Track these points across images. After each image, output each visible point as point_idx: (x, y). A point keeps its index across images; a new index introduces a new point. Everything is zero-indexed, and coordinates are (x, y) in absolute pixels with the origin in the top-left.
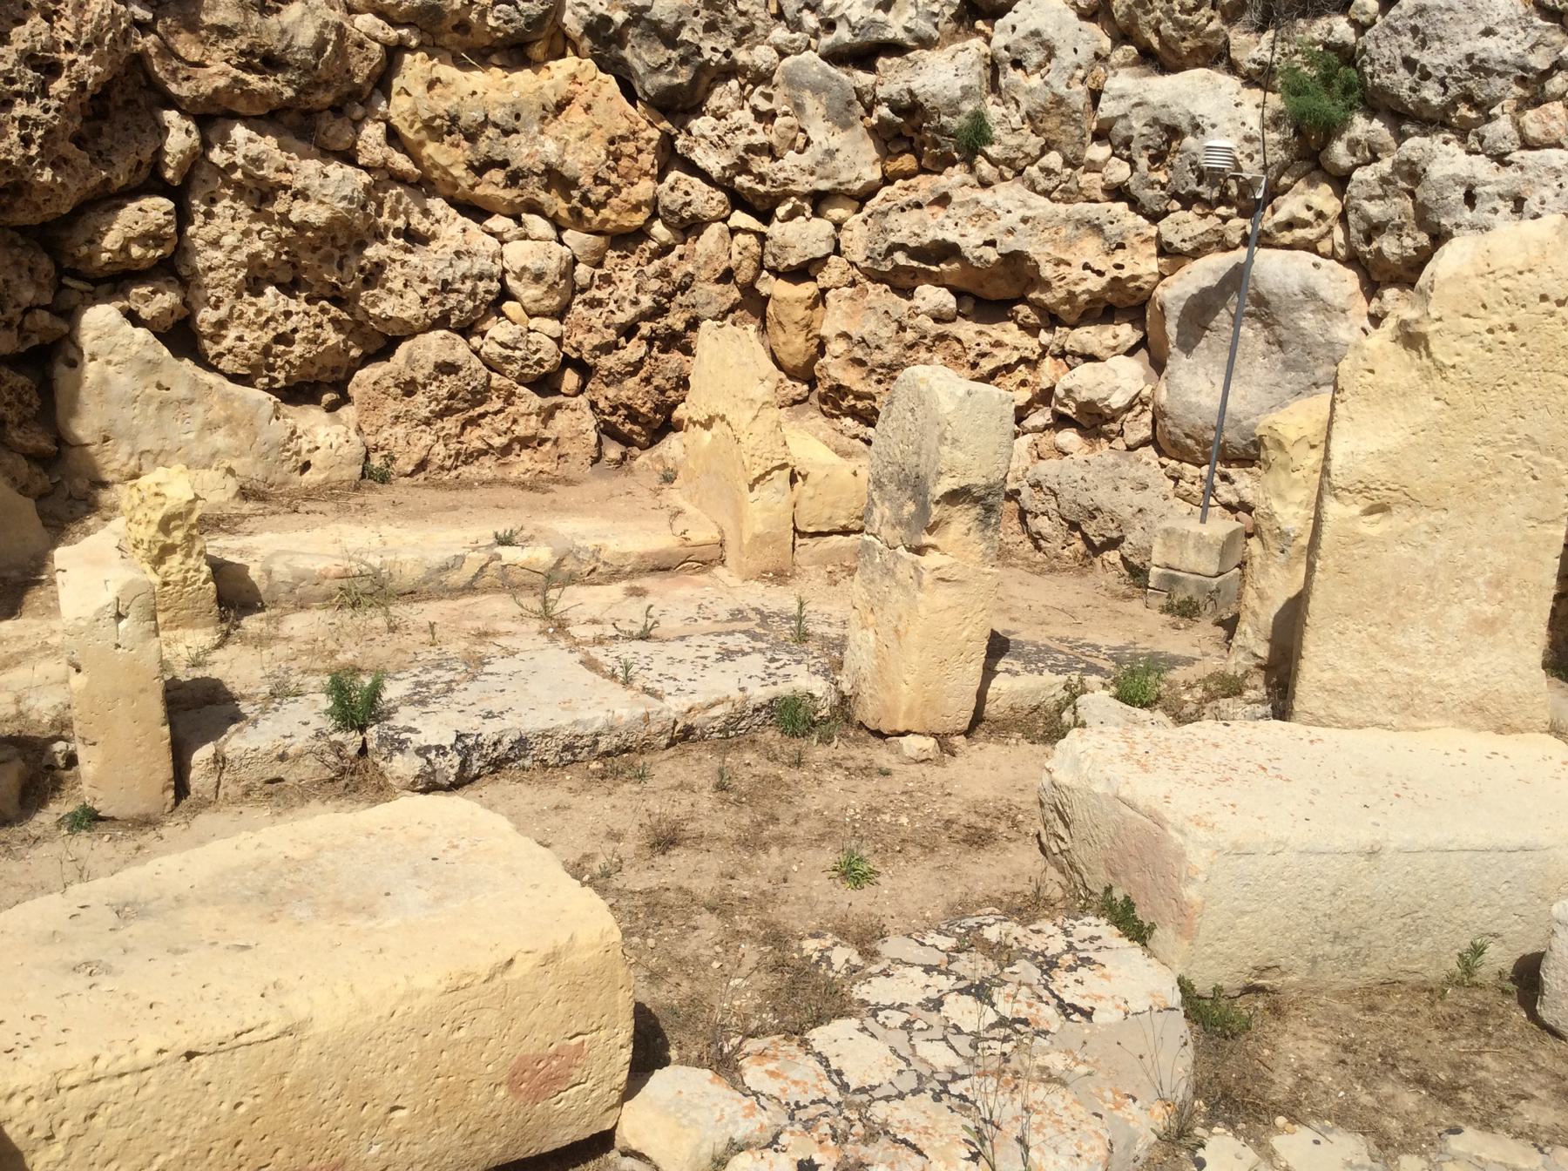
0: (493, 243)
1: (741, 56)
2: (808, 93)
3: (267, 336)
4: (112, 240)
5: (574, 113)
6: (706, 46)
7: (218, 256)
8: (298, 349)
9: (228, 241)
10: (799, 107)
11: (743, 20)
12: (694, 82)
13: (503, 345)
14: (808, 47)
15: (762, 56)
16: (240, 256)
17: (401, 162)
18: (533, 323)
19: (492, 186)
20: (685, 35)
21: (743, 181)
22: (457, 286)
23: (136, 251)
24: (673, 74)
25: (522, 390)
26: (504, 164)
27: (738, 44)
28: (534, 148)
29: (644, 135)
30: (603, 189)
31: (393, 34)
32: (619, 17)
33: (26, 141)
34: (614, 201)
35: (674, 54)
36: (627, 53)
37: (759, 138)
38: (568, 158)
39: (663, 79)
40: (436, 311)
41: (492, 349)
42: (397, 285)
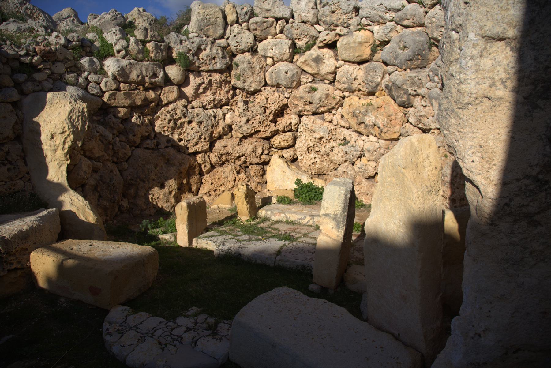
0: (361, 142)
1: (419, 91)
2: (434, 100)
3: (310, 163)
4: (278, 141)
5: (382, 110)
6: (410, 89)
7: (301, 144)
8: (317, 166)
9: (304, 141)
10: (432, 105)
11: (420, 81)
12: (408, 99)
13: (359, 168)
14: (436, 87)
15: (422, 91)
16: (306, 145)
17: (343, 123)
18: (370, 163)
19: (362, 128)
20: (405, 87)
21: (420, 126)
22: (349, 152)
23: (282, 144)
24: (402, 97)
25: (364, 180)
26: (364, 123)
27: (419, 87)
28: (370, 119)
29: (399, 114)
30: (386, 129)
31: (342, 94)
32: (390, 85)
33: (260, 123)
34: (389, 132)
35: (402, 92)
36: (393, 93)
37: (423, 113)
38: (377, 121)
39: (400, 99)
40: (344, 159)
41: (357, 169)
42: (337, 152)
